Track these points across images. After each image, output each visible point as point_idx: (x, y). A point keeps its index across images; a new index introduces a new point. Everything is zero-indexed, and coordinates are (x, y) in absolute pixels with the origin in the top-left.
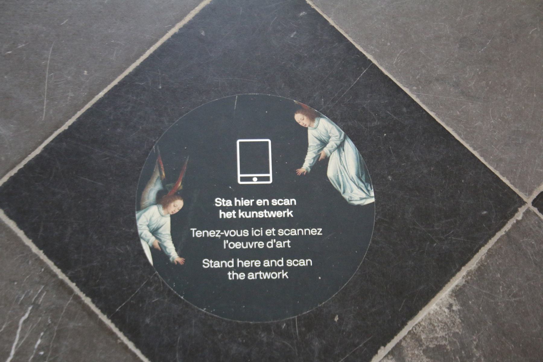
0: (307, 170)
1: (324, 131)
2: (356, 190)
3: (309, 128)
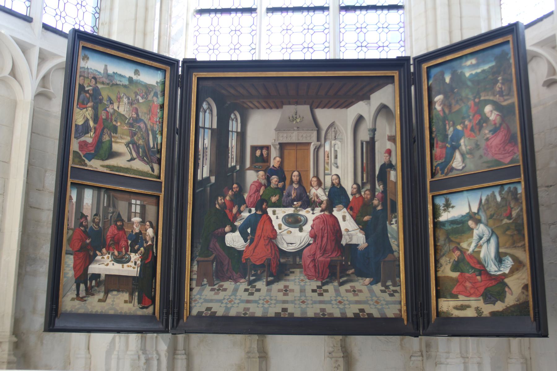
0: (471, 252)
2: (493, 266)
3: (475, 229)
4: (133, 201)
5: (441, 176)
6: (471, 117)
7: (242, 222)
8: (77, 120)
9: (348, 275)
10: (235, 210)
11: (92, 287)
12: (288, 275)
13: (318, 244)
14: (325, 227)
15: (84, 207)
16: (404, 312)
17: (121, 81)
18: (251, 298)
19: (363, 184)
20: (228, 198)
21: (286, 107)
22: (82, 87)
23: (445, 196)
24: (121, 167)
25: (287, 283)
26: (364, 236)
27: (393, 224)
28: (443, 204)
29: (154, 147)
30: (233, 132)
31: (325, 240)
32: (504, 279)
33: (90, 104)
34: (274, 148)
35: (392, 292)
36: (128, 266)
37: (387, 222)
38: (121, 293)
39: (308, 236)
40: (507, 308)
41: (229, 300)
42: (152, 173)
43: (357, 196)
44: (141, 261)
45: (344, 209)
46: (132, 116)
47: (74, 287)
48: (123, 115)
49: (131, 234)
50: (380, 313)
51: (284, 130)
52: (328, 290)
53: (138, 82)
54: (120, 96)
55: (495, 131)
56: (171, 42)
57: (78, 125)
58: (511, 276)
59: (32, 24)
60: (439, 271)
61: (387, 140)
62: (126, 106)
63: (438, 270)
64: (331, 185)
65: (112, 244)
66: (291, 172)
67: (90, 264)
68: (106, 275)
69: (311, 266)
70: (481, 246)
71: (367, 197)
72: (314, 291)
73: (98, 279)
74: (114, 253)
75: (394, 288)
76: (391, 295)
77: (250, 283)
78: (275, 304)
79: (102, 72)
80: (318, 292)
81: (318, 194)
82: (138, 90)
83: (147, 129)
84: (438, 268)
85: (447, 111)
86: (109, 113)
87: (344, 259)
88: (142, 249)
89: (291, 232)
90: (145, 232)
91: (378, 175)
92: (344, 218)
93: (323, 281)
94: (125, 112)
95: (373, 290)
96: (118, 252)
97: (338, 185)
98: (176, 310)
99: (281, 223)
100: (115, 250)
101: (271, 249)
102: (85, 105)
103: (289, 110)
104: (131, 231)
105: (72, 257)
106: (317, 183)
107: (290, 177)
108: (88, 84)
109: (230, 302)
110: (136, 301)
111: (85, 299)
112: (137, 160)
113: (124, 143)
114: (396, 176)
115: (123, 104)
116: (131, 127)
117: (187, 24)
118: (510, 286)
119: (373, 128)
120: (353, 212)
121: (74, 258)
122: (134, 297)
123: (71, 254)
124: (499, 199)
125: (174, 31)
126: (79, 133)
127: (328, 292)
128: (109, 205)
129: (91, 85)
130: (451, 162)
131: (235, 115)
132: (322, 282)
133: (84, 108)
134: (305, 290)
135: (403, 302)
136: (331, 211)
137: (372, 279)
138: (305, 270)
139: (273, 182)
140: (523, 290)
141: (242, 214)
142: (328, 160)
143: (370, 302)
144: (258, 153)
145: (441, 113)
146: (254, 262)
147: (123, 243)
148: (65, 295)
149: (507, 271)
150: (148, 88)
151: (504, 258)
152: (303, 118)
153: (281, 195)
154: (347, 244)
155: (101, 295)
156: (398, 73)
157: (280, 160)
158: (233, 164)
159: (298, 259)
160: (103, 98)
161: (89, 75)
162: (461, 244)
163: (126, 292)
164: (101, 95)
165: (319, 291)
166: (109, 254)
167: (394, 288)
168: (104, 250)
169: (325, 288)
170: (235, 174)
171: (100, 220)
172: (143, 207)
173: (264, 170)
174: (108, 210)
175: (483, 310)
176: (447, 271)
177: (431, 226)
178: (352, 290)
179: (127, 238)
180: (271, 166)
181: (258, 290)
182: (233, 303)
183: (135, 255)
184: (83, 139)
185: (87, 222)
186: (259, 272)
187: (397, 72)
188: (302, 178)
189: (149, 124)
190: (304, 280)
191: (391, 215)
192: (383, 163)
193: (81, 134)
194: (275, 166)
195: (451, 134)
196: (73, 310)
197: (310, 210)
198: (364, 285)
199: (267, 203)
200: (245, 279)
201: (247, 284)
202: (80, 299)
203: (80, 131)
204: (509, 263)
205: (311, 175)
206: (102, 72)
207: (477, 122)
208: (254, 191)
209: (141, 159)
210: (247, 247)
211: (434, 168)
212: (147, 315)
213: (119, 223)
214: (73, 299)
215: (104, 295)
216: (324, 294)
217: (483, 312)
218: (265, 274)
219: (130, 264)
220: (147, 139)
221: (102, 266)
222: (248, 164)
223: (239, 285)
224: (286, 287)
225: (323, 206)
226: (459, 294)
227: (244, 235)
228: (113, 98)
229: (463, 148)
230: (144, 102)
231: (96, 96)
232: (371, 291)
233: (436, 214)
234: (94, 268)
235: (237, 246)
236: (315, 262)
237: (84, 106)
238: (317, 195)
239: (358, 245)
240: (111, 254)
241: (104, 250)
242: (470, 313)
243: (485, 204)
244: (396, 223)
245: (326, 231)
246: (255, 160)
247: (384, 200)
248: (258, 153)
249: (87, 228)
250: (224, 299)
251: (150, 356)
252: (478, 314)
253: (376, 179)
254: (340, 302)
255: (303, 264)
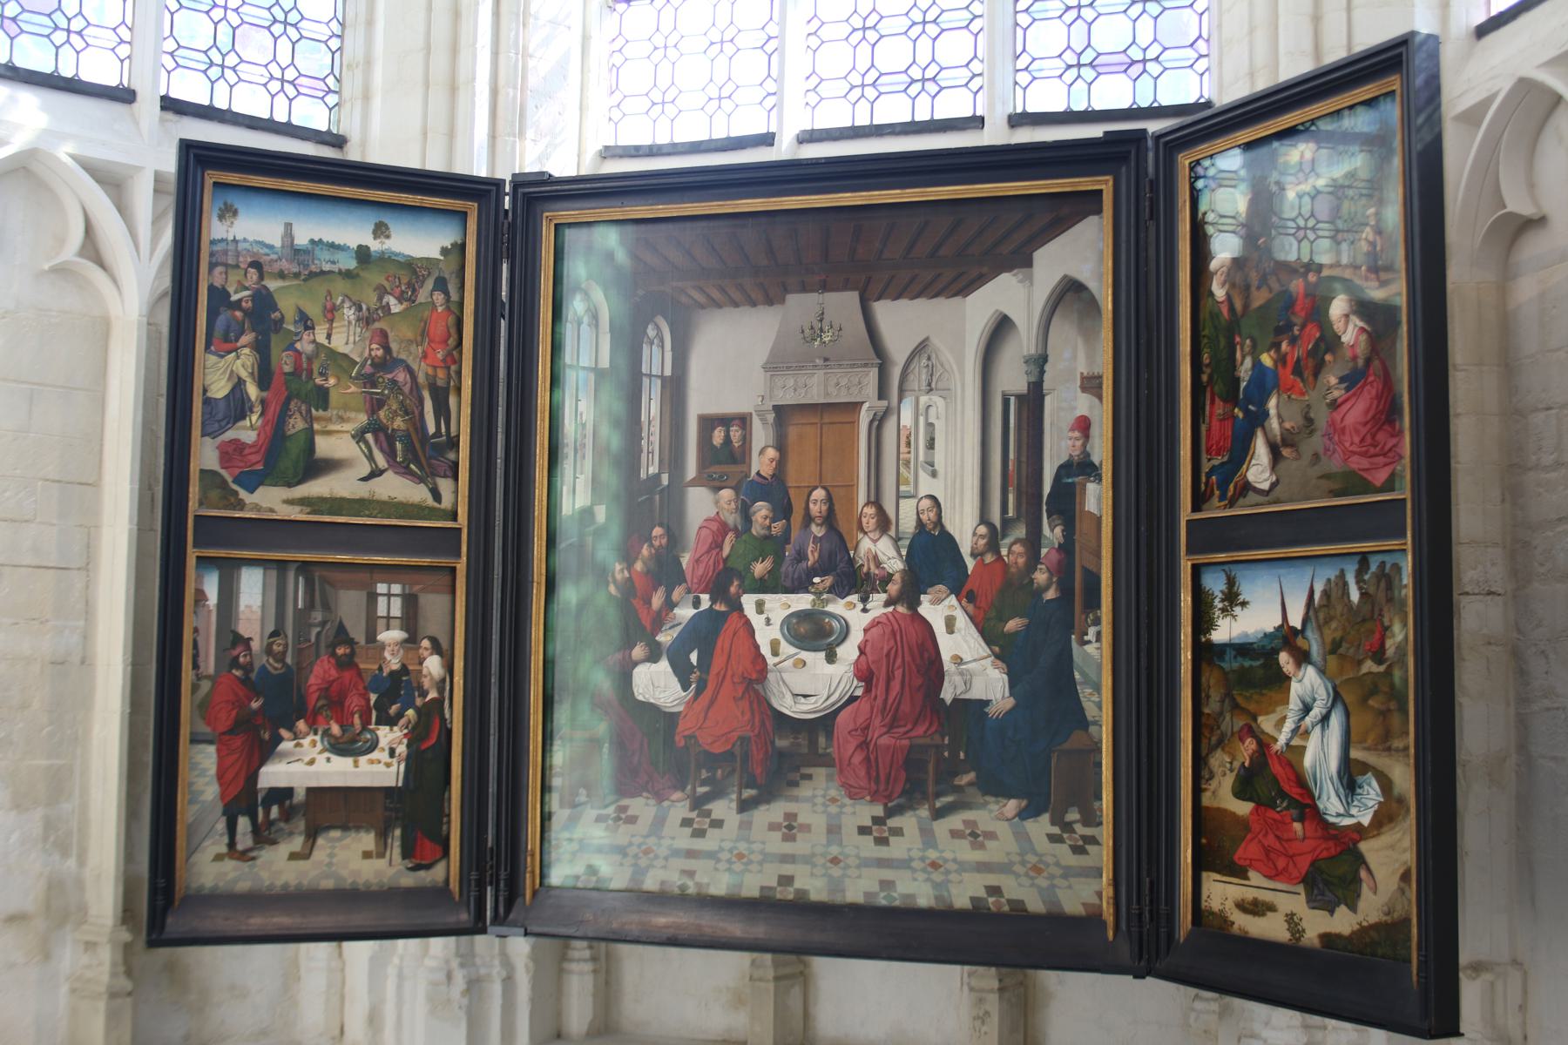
0: (1282, 748)
1: (1309, 687)
2: (1334, 799)
3: (1294, 679)
4: (381, 588)
5: (1218, 504)
6: (1296, 331)
7: (675, 633)
8: (212, 387)
9: (959, 789)
10: (657, 600)
11: (270, 823)
12: (795, 784)
13: (876, 697)
14: (897, 651)
15: (242, 616)
16: (1108, 903)
17: (333, 263)
18: (699, 844)
19: (1006, 523)
20: (639, 566)
21: (794, 300)
22: (219, 297)
23: (1226, 567)
24: (343, 499)
25: (791, 807)
26: (1005, 677)
27: (1089, 642)
28: (1222, 592)
29: (438, 433)
30: (653, 378)
31: (896, 686)
32: (1358, 842)
33: (247, 338)
34: (761, 420)
35: (1081, 843)
36: (372, 762)
37: (1073, 637)
38: (353, 834)
39: (851, 674)
40: (1363, 931)
41: (644, 847)
42: (436, 505)
43: (989, 558)
44: (408, 746)
45: (948, 599)
46: (370, 355)
47: (221, 825)
48: (345, 356)
49: (376, 675)
50: (1044, 902)
51: (788, 368)
52: (901, 829)
53: (386, 256)
54: (334, 305)
55: (1352, 380)
56: (530, 105)
57: (216, 399)
58: (1374, 836)
59: (135, 105)
60: (1205, 790)
61: (1079, 390)
62: (352, 328)
63: (1204, 786)
64: (916, 528)
65: (323, 706)
66: (806, 491)
67: (262, 763)
68: (310, 791)
69: (857, 759)
70: (1307, 733)
71: (1016, 563)
72: (863, 830)
73: (288, 803)
74: (329, 729)
75: (1088, 831)
76: (1078, 850)
77: (698, 803)
78: (761, 863)
79: (277, 243)
80: (875, 834)
81: (880, 555)
82: (387, 279)
83: (417, 383)
84: (1203, 781)
85: (1238, 305)
86: (303, 355)
87: (946, 742)
88: (410, 712)
89: (805, 664)
90: (417, 668)
91: (1049, 495)
92: (950, 625)
93: (890, 805)
94: (351, 346)
95: (1027, 834)
96: (341, 726)
97: (934, 528)
98: (503, 875)
99: (779, 636)
100: (332, 722)
101: (753, 714)
102: (231, 342)
103: (801, 306)
104: (376, 667)
105: (211, 749)
106: (878, 521)
107: (803, 505)
108: (239, 282)
109: (647, 852)
110: (397, 851)
111: (253, 854)
112: (389, 475)
113: (347, 432)
114: (1099, 499)
115: (343, 326)
116: (368, 386)
117: (586, 39)
118: (1373, 866)
119: (1039, 352)
120: (975, 606)
121: (218, 751)
122: (390, 841)
123: (210, 742)
124: (1355, 596)
125: (538, 70)
126: (219, 421)
127: (903, 835)
128: (310, 605)
129: (247, 285)
130: (1245, 466)
131: (658, 328)
132: (885, 805)
133: (229, 352)
134: (840, 827)
135: (1107, 875)
136: (914, 604)
137: (1024, 803)
138: (841, 771)
139: (757, 521)
140: (1403, 885)
141: (677, 611)
142: (909, 452)
143: (1018, 868)
144: (718, 436)
145: (1225, 310)
146: (707, 748)
147: (354, 702)
148: (197, 848)
149: (1366, 820)
150: (413, 269)
151: (1360, 779)
152: (841, 329)
153: (779, 558)
154: (955, 700)
155: (297, 843)
156: (1111, 183)
157: (778, 454)
158: (653, 470)
159: (822, 740)
160: (282, 315)
161: (241, 259)
162: (1260, 719)
163: (368, 831)
164: (275, 308)
165: (876, 829)
166: (316, 734)
167: (1088, 831)
168: (301, 725)
169: (893, 822)
170: (657, 497)
171: (286, 646)
172: (410, 602)
173: (734, 484)
174: (310, 618)
175: (1304, 924)
176: (1224, 796)
177: (1186, 656)
178: (968, 831)
179: (365, 688)
180: (753, 472)
181: (718, 824)
182: (651, 855)
183: (391, 730)
184: (230, 435)
185: (251, 654)
186: (719, 772)
187: (1109, 178)
188: (837, 507)
189: (422, 371)
190: (838, 801)
191: (1083, 617)
192: (1064, 458)
193: (223, 423)
194: (762, 473)
195: (1247, 378)
196: (221, 884)
197: (856, 602)
198: (1001, 817)
199: (741, 578)
200: (683, 791)
201: (688, 806)
202: (237, 855)
203: (220, 416)
204: (1371, 794)
205: (862, 498)
206: (277, 243)
207: (1310, 347)
208: (705, 548)
209: (403, 470)
210: (689, 704)
211: (1204, 479)
212: (429, 885)
213: (340, 651)
214: (219, 858)
215: (306, 842)
216: (892, 839)
217: (1304, 931)
218: (735, 779)
219: (375, 755)
220: (416, 412)
221: (298, 767)
222: (691, 470)
223: (669, 807)
224: (790, 817)
225: (893, 588)
226: (1250, 866)
227: (682, 672)
228: (313, 310)
229: (1274, 424)
230: (406, 309)
231: (262, 311)
232: (1022, 837)
233: (1202, 622)
234: (273, 774)
235: (662, 700)
236: (868, 750)
237: (228, 346)
238: (876, 557)
239: (987, 703)
240: (320, 733)
241: (301, 725)
242: (1271, 928)
243: (1321, 606)
244: (1097, 641)
245: (899, 661)
246: (709, 456)
247: (1064, 572)
248: (718, 436)
249: (252, 670)
250: (631, 844)
251: (483, 971)
252: (1293, 935)
253: (1045, 508)
254: (935, 865)
255: (835, 756)
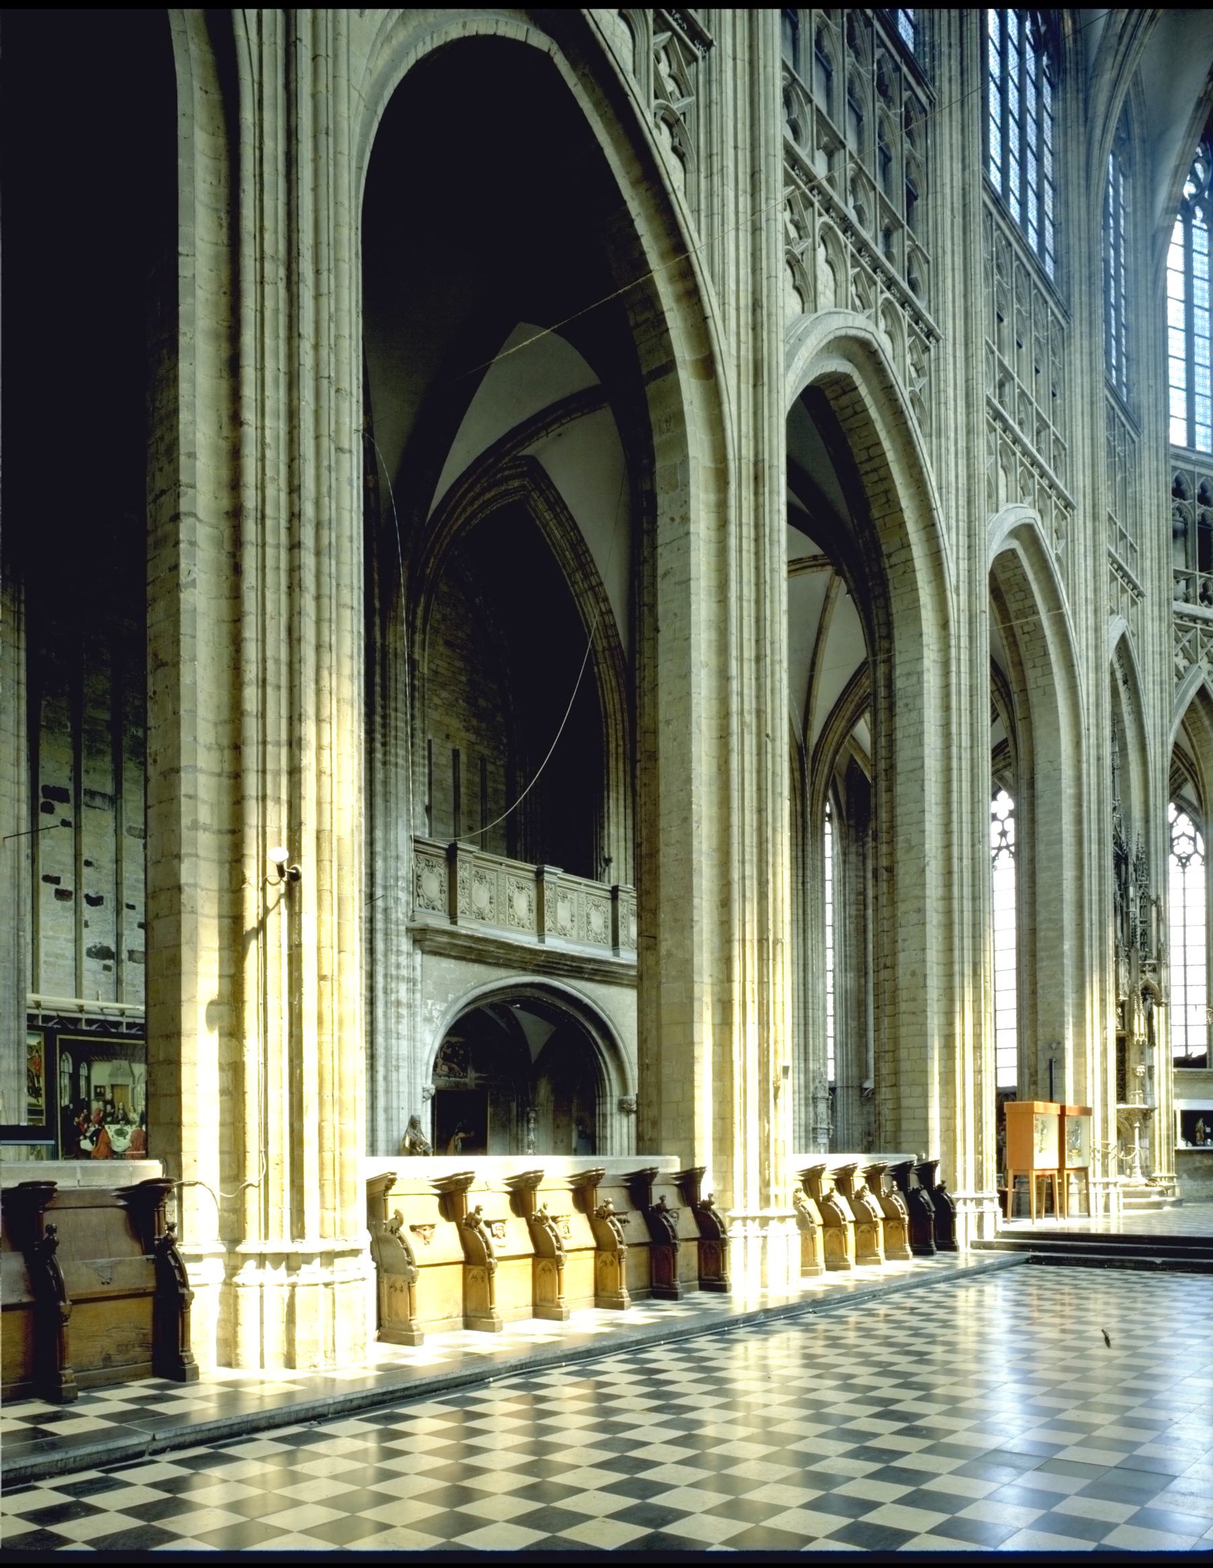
103: (116, 1063)
227: (92, 1142)
246: (97, 1094)
